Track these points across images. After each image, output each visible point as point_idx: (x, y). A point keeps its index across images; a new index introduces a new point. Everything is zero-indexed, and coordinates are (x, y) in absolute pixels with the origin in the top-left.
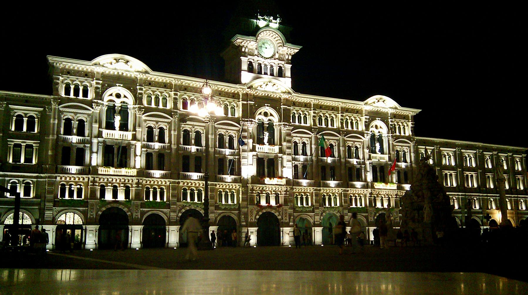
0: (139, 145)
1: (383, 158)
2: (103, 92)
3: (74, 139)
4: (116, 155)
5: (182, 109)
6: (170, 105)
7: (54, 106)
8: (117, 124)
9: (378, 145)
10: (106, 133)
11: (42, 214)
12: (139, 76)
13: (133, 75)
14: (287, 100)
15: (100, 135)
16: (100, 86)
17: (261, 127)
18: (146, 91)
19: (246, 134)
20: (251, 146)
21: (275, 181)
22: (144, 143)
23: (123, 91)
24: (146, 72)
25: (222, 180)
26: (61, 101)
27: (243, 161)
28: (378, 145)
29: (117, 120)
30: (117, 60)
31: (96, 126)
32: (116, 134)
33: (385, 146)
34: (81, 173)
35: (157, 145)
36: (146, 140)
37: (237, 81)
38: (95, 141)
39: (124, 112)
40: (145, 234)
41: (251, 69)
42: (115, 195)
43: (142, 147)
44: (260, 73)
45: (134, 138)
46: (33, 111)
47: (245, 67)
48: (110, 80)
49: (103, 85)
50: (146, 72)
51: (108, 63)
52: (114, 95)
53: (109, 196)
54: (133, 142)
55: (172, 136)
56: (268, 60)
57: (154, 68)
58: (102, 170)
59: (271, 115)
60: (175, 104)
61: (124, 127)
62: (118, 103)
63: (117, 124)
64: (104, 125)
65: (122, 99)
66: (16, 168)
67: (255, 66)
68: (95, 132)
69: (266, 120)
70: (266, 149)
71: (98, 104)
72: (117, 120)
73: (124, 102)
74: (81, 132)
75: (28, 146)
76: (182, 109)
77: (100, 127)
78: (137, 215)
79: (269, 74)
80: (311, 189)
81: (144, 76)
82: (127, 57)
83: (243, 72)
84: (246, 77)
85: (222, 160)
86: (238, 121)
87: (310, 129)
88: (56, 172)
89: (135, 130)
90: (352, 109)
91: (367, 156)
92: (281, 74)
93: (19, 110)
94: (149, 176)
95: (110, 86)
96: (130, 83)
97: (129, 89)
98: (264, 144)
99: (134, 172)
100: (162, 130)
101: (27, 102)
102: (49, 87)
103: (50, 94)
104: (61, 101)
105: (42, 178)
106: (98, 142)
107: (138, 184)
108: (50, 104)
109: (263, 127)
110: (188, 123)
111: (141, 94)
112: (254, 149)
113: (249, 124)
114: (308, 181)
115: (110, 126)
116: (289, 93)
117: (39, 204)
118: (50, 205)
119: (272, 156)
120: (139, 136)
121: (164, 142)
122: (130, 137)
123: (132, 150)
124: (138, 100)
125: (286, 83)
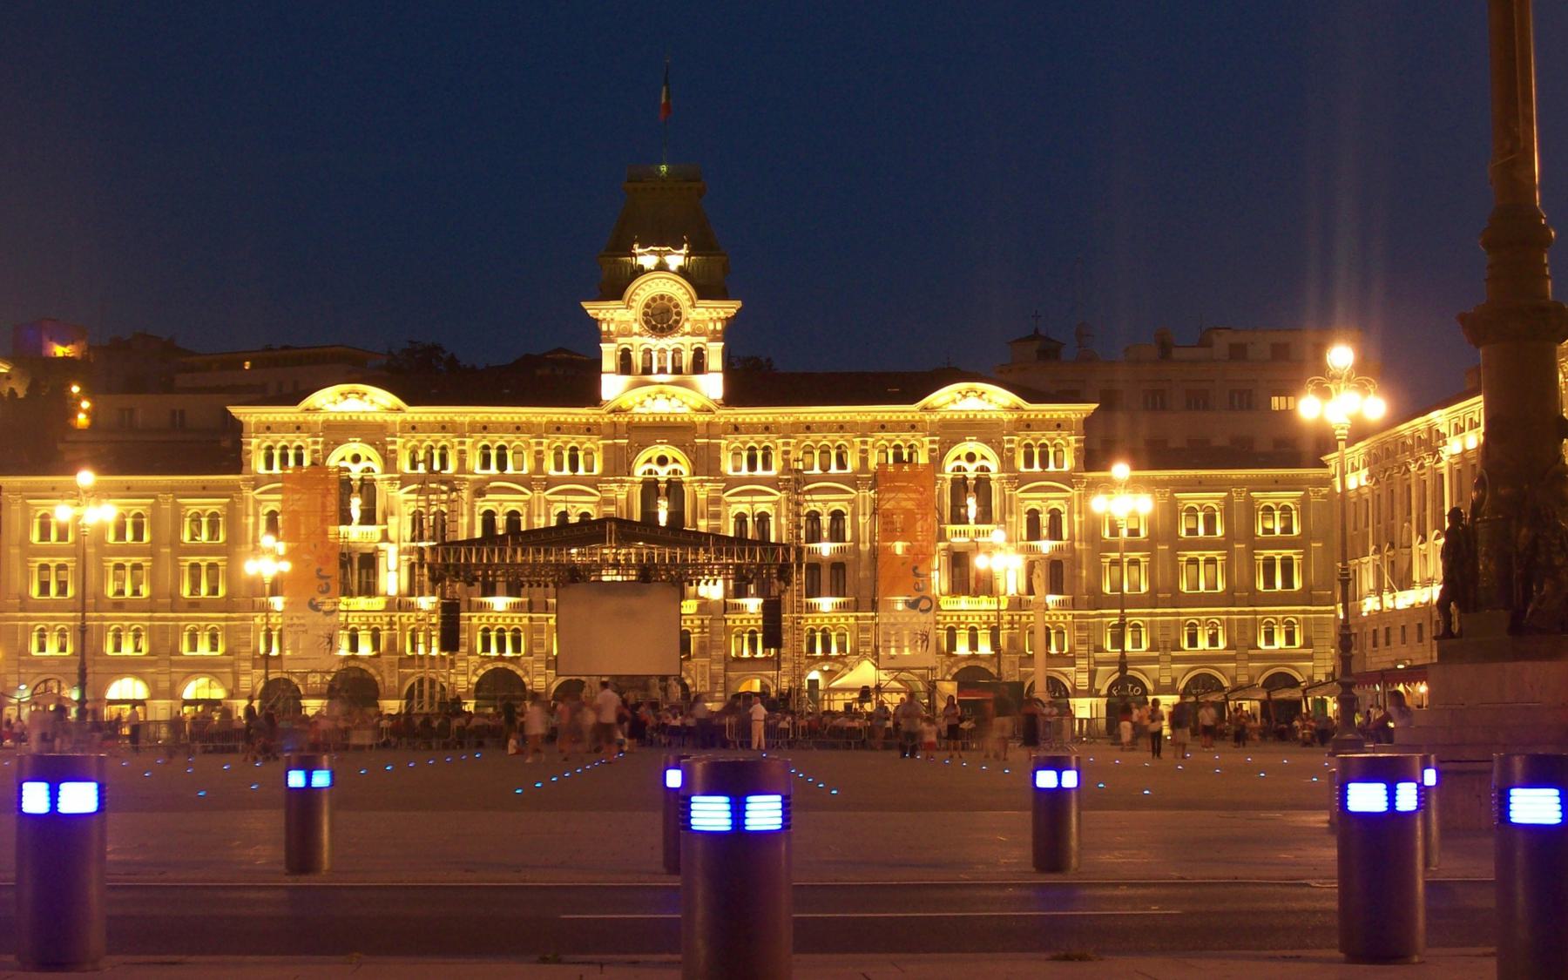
5: (478, 470)
6: (528, 466)
8: (356, 512)
9: (972, 502)
11: (236, 681)
12: (390, 418)
13: (379, 418)
14: (709, 424)
16: (319, 447)
21: (361, 602)
22: (403, 545)
23: (365, 450)
24: (399, 410)
26: (257, 482)
28: (972, 502)
29: (356, 505)
30: (344, 395)
33: (996, 501)
36: (408, 537)
37: (591, 397)
39: (982, 487)
41: (625, 365)
43: (400, 553)
45: (385, 537)
46: (214, 505)
47: (609, 361)
49: (326, 444)
50: (399, 410)
52: (348, 458)
53: (344, 650)
54: (382, 546)
57: (412, 400)
59: (675, 461)
60: (539, 460)
61: (369, 518)
63: (356, 512)
65: (363, 464)
66: (194, 605)
67: (637, 359)
69: (663, 473)
72: (356, 505)
73: (675, 471)
75: (212, 566)
79: (669, 369)
80: (1068, 616)
81: (398, 418)
83: (603, 377)
84: (613, 386)
86: (594, 483)
88: (253, 609)
89: (385, 522)
92: (699, 365)
93: (193, 505)
94: (410, 608)
95: (338, 444)
96: (375, 434)
97: (372, 444)
99: (378, 603)
101: (205, 491)
102: (233, 460)
103: (239, 472)
104: (257, 482)
105: (233, 619)
107: (391, 623)
108: (238, 489)
109: (658, 490)
110: (489, 497)
111: (394, 451)
116: (709, 411)
117: (231, 664)
118: (246, 665)
120: (392, 534)
121: (1061, 539)
122: (378, 536)
124: (389, 462)
125: (712, 385)
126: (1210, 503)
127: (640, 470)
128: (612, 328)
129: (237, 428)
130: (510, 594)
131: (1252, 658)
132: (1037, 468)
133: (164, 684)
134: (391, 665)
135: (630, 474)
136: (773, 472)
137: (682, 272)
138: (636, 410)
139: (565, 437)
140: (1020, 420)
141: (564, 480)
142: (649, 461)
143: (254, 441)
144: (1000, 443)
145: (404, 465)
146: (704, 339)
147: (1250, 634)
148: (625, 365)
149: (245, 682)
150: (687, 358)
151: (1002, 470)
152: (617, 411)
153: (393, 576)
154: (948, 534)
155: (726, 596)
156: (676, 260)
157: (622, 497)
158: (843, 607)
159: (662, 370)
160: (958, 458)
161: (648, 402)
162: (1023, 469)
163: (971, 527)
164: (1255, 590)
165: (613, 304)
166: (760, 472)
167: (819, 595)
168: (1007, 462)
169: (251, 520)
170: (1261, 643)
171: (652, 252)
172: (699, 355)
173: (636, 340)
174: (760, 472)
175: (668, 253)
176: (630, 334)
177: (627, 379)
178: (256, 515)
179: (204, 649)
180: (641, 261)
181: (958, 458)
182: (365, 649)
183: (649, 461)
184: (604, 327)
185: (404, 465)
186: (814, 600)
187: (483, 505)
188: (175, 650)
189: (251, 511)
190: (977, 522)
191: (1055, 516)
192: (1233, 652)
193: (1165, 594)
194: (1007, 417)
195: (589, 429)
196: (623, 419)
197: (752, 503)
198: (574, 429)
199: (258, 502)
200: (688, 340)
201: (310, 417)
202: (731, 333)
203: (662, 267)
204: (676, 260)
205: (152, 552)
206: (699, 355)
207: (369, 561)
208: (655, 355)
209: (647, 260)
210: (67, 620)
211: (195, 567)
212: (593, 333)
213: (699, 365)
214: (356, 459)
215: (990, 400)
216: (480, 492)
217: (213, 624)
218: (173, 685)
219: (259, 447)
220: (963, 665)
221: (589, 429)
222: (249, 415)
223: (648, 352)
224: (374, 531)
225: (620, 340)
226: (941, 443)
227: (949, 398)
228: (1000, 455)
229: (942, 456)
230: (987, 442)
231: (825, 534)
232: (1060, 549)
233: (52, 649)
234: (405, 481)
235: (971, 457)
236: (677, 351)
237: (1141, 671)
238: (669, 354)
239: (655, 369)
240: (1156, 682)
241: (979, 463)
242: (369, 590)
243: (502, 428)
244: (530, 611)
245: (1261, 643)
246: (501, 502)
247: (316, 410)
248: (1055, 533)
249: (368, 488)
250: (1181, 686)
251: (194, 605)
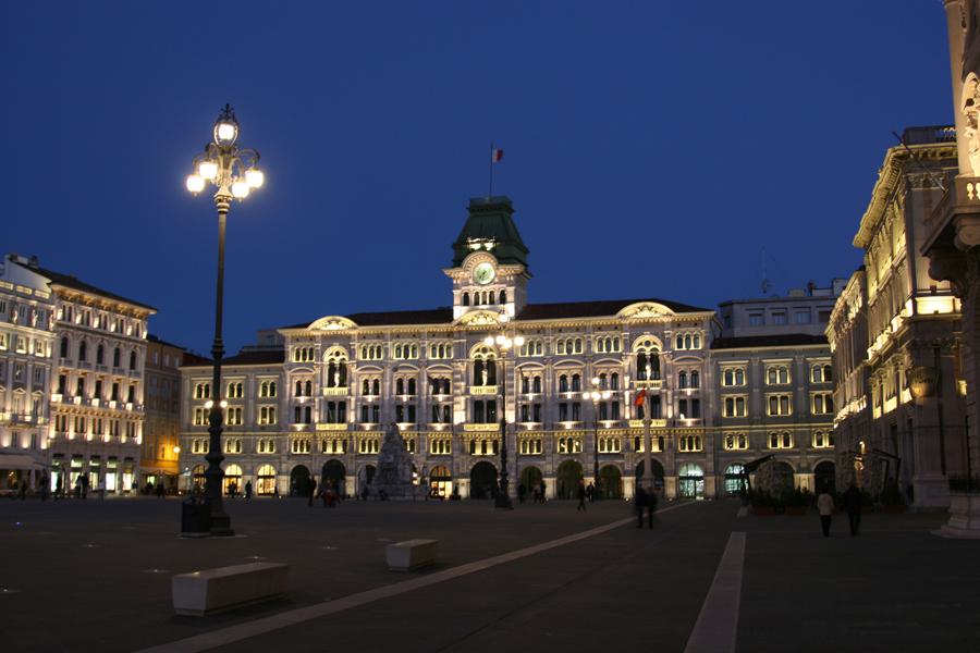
0: (353, 399)
1: (658, 385)
2: (323, 353)
3: (302, 399)
4: (336, 410)
5: (395, 358)
7: (289, 373)
10: (327, 391)
12: (352, 332)
15: (321, 393)
17: (478, 365)
18: (356, 345)
19: (459, 376)
20: (463, 389)
23: (342, 350)
25: (432, 429)
26: (291, 366)
27: (455, 406)
30: (330, 322)
31: (318, 386)
32: (337, 391)
33: (662, 367)
34: (615, 426)
35: (370, 398)
37: (446, 315)
38: (317, 400)
40: (360, 483)
41: (466, 301)
42: (484, 450)
44: (477, 303)
45: (350, 393)
46: (271, 379)
47: (457, 301)
48: (330, 339)
50: (355, 328)
51: (323, 325)
55: (389, 387)
56: (488, 287)
58: (318, 427)
62: (337, 360)
63: (337, 381)
64: (326, 382)
65: (341, 357)
67: (472, 298)
68: (318, 391)
69: (485, 357)
70: (485, 390)
71: (318, 366)
74: (308, 393)
76: (395, 358)
77: (321, 386)
78: (628, 467)
82: (338, 318)
84: (459, 312)
85: (436, 407)
86: (449, 362)
87: (542, 360)
90: (608, 326)
91: (627, 386)
92: (503, 300)
94: (362, 429)
95: (329, 346)
96: (344, 339)
98: (480, 383)
100: (376, 382)
101: (269, 371)
102: (279, 356)
106: (320, 400)
108: (283, 371)
112: (467, 392)
113: (459, 364)
114: (574, 423)
115: (331, 384)
118: (284, 459)
119: (490, 399)
120: (354, 391)
123: (348, 405)
124: (351, 354)
125: (510, 309)
126: (783, 365)
127: (473, 356)
128: (459, 282)
129: (283, 338)
130: (410, 422)
131: (809, 453)
132: (684, 348)
133: (249, 468)
134: (352, 458)
135: (468, 357)
136: (542, 355)
137: (493, 251)
138: (470, 324)
139: (436, 340)
140: (673, 322)
141: (436, 362)
142: (478, 351)
143: (291, 347)
144: (663, 335)
145: (359, 356)
146: (505, 286)
147: (807, 439)
148: (466, 301)
149: (284, 466)
150: (497, 296)
151: (663, 350)
152: (460, 324)
153: (353, 413)
154: (635, 386)
155: (517, 421)
156: (489, 246)
157: (463, 370)
158: (576, 426)
159: (484, 303)
160: (641, 344)
161: (476, 319)
162: (676, 349)
163: (648, 382)
164: (765, 415)
165: (456, 270)
166: (535, 355)
167: (564, 420)
168: (666, 344)
169: (288, 386)
170: (815, 445)
171: (478, 242)
172: (503, 294)
173: (471, 288)
174: (535, 355)
175: (486, 242)
176: (467, 284)
177: (466, 308)
178: (291, 382)
179: (267, 451)
180: (472, 246)
181: (641, 344)
182: (340, 450)
183: (478, 351)
184: (455, 282)
185: (359, 356)
186: (563, 423)
187: (397, 376)
188: (254, 451)
189: (288, 380)
190: (651, 379)
191: (412, 382)
192: (797, 450)
193: (757, 418)
194: (666, 320)
195: (450, 335)
196: (462, 328)
197: (608, 368)
198: (441, 335)
199: (292, 377)
200: (497, 286)
201: (315, 333)
202: (519, 281)
203: (483, 249)
204: (489, 246)
205: (245, 403)
206: (503, 294)
207: (343, 405)
208: (480, 295)
209: (476, 246)
210: (206, 437)
211: (264, 409)
212: (449, 285)
213: (503, 300)
214: (337, 354)
215: (659, 312)
216: (395, 370)
217: (271, 438)
218: (253, 468)
219: (293, 349)
220: (478, 461)
221: (450, 335)
222: (288, 333)
223: (477, 293)
224: (345, 390)
225: (463, 288)
226: (631, 336)
227: (633, 311)
228: (663, 342)
229: (632, 343)
230: (656, 335)
231: (569, 387)
232: (697, 392)
233: (201, 451)
234: (359, 364)
235: (648, 344)
236: (492, 293)
237: (789, 459)
238: (488, 294)
239: (481, 302)
240: (799, 465)
241: (652, 347)
242: (342, 420)
243: (406, 335)
244: (545, 429)
245: (815, 445)
246: (405, 374)
247: (318, 329)
248: (694, 384)
249: (343, 368)
250: (813, 468)
251: (263, 428)
